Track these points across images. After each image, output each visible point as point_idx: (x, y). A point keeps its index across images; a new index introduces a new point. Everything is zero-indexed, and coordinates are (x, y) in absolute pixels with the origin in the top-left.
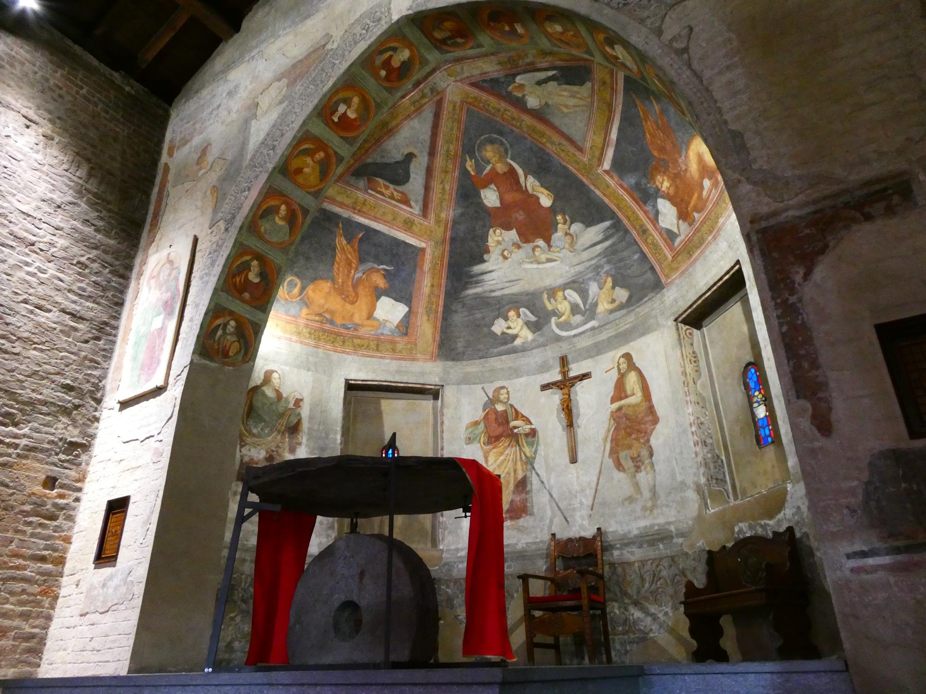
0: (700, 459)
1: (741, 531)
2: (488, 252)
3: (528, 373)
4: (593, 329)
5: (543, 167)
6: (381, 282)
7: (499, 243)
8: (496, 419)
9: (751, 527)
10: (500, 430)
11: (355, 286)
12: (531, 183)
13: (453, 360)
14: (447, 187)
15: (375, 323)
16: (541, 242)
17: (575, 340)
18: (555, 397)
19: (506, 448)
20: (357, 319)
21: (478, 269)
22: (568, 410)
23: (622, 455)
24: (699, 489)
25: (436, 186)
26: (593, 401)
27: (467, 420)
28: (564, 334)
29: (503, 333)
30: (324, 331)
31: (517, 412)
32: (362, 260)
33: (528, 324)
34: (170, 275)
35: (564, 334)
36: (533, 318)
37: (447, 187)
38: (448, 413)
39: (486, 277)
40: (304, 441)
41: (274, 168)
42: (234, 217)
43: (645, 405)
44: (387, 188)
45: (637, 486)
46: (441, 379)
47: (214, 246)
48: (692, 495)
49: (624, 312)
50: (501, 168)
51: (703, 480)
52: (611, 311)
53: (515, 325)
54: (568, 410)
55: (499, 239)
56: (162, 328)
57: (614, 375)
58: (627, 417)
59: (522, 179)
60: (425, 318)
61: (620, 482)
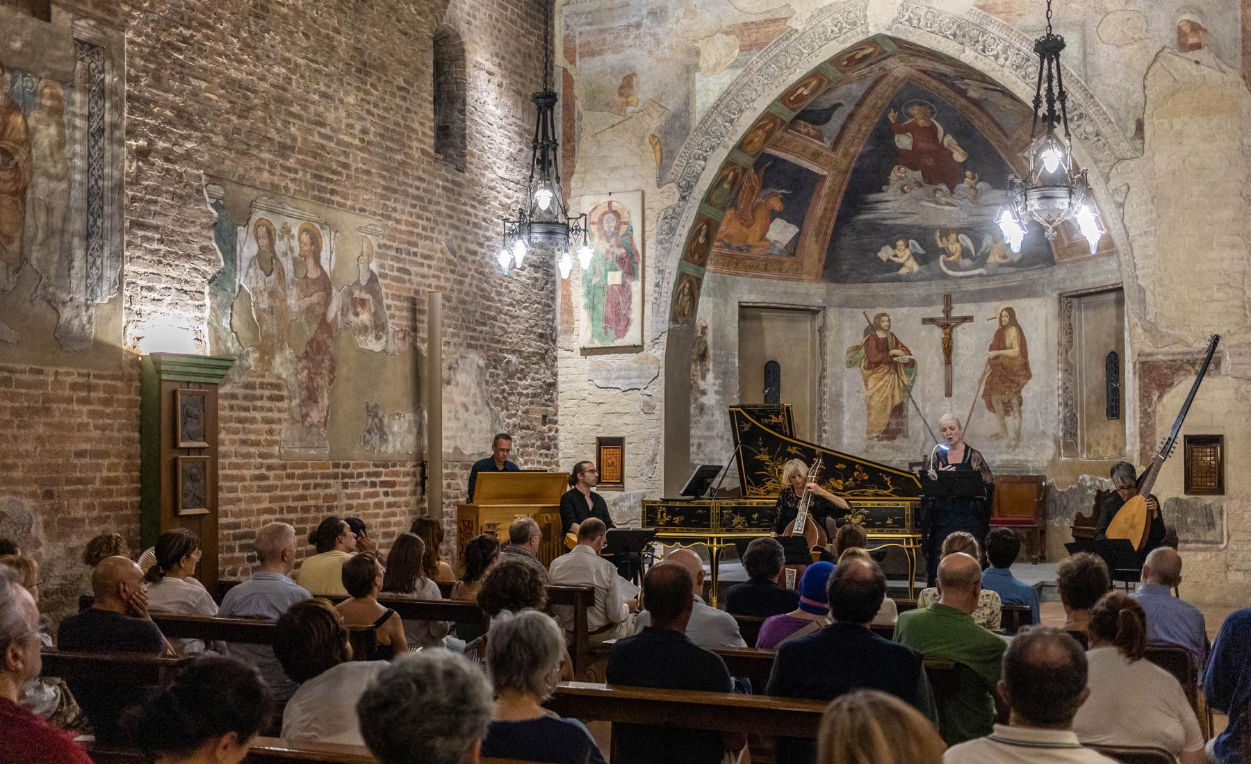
0: (1061, 416)
1: (1084, 479)
2: (887, 183)
3: (911, 305)
4: (981, 275)
5: (965, 134)
6: (776, 204)
7: (901, 178)
8: (877, 346)
9: (1091, 479)
10: (880, 356)
11: (753, 211)
12: (948, 140)
13: (837, 282)
14: (864, 129)
15: (766, 244)
16: (944, 187)
17: (962, 281)
18: (938, 333)
19: (885, 375)
20: (750, 241)
21: (873, 197)
22: (948, 349)
23: (994, 398)
24: (1056, 441)
25: (853, 127)
26: (973, 344)
27: (848, 344)
28: (951, 273)
29: (889, 260)
30: (722, 255)
31: (897, 342)
32: (764, 186)
33: (915, 255)
34: (618, 228)
35: (951, 273)
36: (921, 251)
37: (864, 129)
38: (831, 336)
39: (879, 205)
40: (711, 367)
41: (734, 147)
42: (690, 187)
43: (1020, 361)
44: (805, 127)
45: (1004, 426)
46: (824, 301)
47: (670, 211)
48: (1050, 444)
49: (1012, 269)
50: (922, 123)
51: (1061, 434)
52: (1001, 265)
53: (903, 255)
54: (948, 349)
55: (898, 173)
56: (623, 285)
57: (997, 327)
58: (1004, 367)
59: (940, 136)
60: (814, 239)
61: (988, 422)
